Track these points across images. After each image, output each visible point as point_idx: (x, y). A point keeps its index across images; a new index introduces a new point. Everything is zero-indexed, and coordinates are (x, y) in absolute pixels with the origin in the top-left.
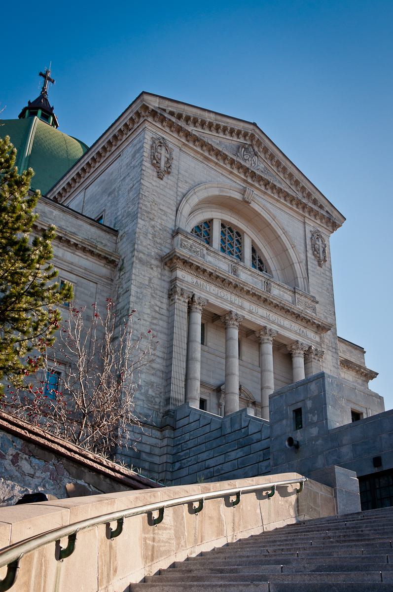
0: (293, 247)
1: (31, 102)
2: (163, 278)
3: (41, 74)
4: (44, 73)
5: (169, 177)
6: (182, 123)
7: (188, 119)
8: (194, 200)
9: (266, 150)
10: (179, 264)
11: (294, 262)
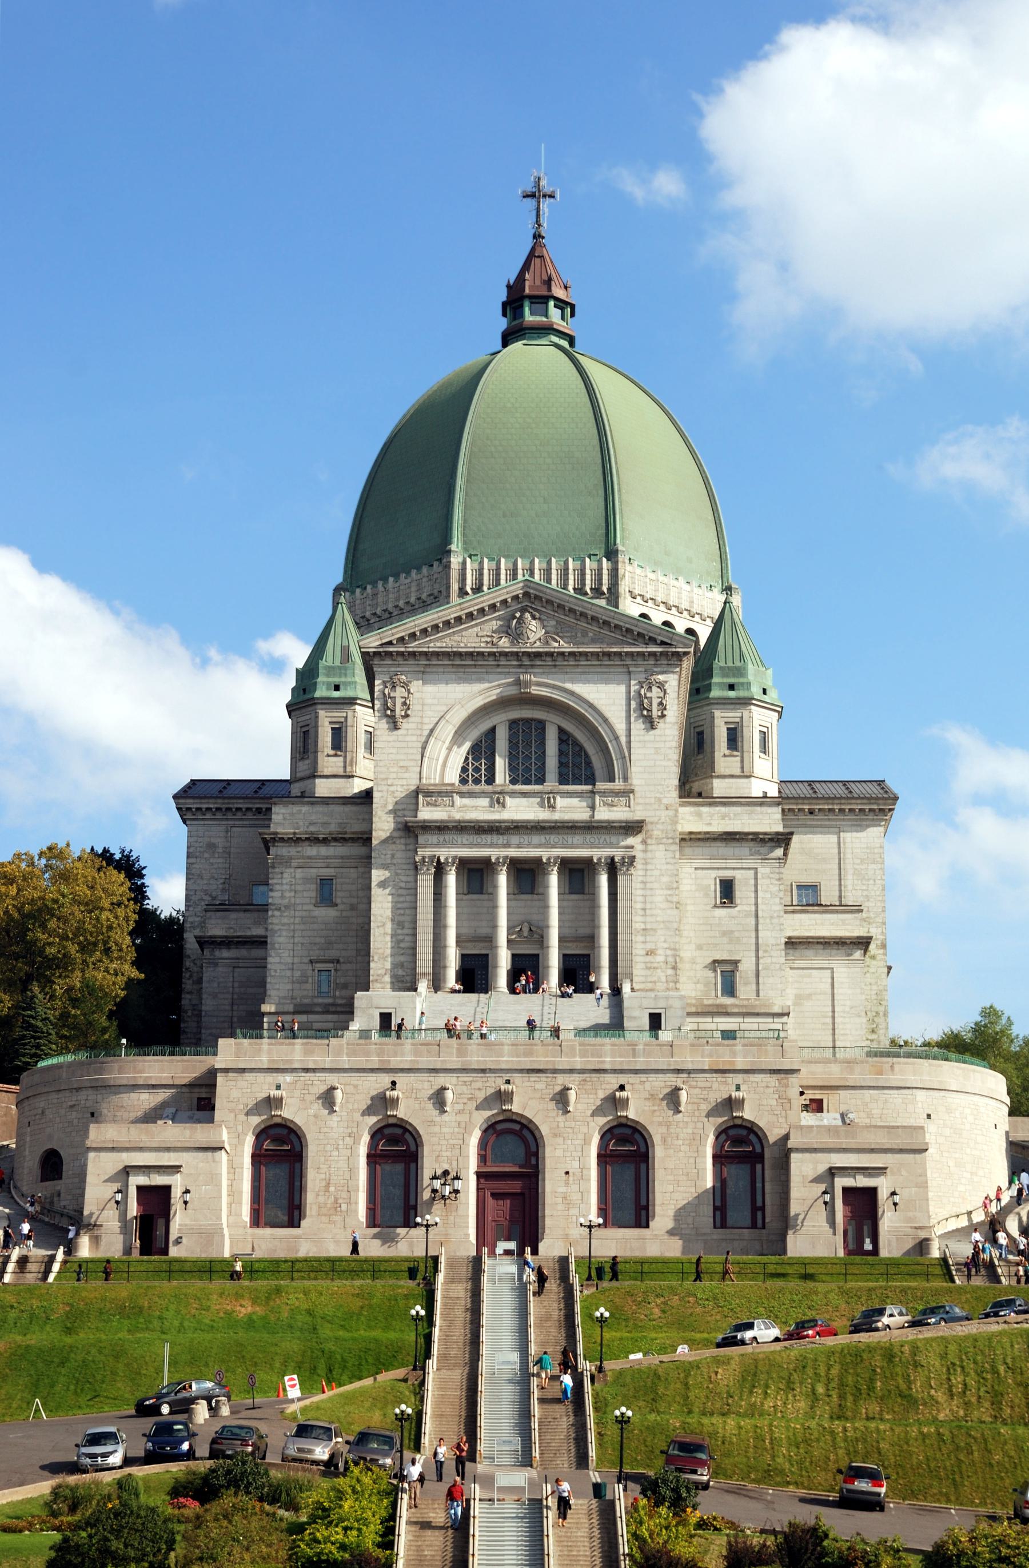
0: (606, 720)
1: (512, 282)
2: (409, 847)
4: (530, 188)
5: (410, 719)
6: (413, 646)
10: (418, 831)
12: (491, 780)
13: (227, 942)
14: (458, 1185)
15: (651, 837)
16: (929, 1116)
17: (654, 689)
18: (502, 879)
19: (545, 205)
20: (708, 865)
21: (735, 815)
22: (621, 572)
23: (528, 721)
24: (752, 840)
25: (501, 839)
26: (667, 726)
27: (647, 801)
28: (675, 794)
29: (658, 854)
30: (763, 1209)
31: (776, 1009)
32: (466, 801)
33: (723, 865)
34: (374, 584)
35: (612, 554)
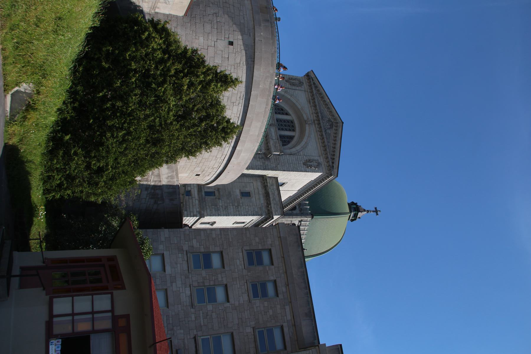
4: (378, 209)
5: (289, 85)
6: (313, 86)
7: (318, 91)
8: (289, 97)
9: (336, 130)
11: (296, 148)
15: (264, 160)
16: (231, 43)
17: (316, 164)
19: (375, 213)
20: (255, 187)
21: (275, 198)
22: (307, 216)
23: (293, 126)
24: (267, 203)
26: (305, 168)
27: (278, 160)
29: (259, 162)
31: (202, 212)
33: (256, 193)
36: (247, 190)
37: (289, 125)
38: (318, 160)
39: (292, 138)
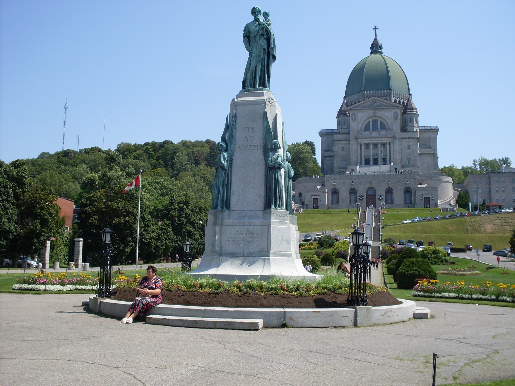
3: (374, 29)
4: (374, 28)
6: (356, 108)
8: (362, 122)
9: (378, 100)
12: (369, 129)
13: (328, 157)
14: (363, 197)
18: (371, 146)
19: (377, 30)
25: (371, 140)
28: (400, 131)
30: (412, 200)
32: (365, 134)
34: (350, 96)
35: (390, 89)
36: (407, 146)
37: (375, 122)
38: (394, 113)
39: (381, 122)
